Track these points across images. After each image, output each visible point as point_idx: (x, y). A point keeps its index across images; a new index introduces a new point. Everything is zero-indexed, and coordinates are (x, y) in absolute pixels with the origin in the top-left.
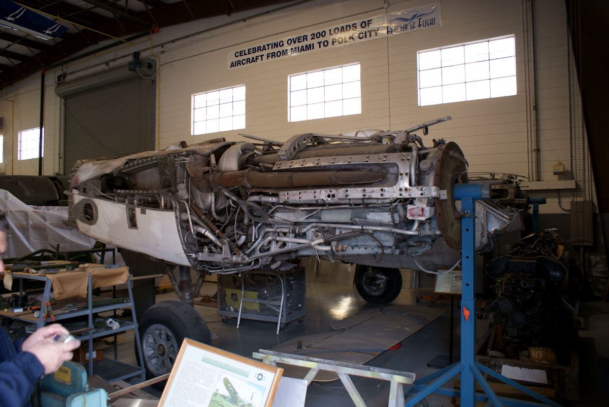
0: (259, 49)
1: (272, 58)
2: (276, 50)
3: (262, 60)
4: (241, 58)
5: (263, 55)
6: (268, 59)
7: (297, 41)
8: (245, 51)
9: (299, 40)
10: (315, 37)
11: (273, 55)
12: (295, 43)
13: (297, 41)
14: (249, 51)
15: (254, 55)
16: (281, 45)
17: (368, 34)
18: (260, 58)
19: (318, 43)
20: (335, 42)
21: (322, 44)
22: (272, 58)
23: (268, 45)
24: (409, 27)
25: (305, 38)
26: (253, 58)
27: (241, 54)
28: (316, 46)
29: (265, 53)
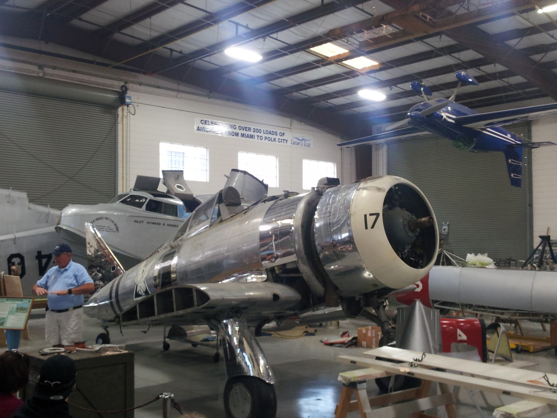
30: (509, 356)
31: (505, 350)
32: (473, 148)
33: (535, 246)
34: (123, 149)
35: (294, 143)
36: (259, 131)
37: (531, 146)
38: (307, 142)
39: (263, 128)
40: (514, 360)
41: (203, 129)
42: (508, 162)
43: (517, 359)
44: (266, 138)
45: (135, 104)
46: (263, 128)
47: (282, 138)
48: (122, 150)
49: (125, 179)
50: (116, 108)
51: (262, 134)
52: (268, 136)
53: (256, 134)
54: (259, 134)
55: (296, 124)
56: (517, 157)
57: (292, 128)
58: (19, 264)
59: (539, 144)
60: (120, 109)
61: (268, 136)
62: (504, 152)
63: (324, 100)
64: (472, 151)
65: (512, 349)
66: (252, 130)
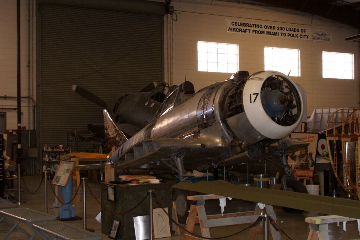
0: (247, 25)
1: (256, 33)
2: (258, 29)
3: (249, 33)
4: (236, 27)
5: (250, 30)
6: (253, 33)
7: (270, 28)
8: (238, 23)
9: (270, 27)
10: (279, 29)
11: (256, 32)
13: (270, 28)
14: (241, 24)
15: (245, 28)
16: (261, 27)
17: (304, 36)
18: (248, 31)
19: (308, 36)
20: (289, 35)
21: (283, 34)
22: (256, 33)
23: (253, 25)
24: (320, 39)
25: (274, 28)
26: (244, 29)
27: (236, 24)
28: (251, 31)
29: (252, 29)
36: (283, 29)
38: (326, 37)
44: (289, 35)
45: (177, 13)
47: (303, 34)
49: (169, 73)
50: (161, 17)
51: (285, 31)
53: (280, 32)
54: (282, 31)
57: (312, 25)
60: (165, 17)
66: (276, 28)
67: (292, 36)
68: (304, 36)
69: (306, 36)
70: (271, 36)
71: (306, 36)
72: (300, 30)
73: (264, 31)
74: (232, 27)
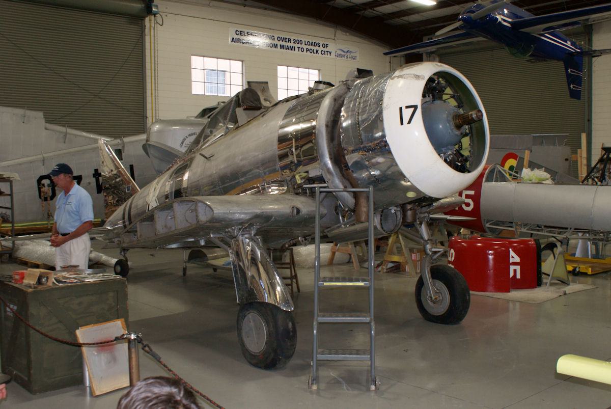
9: (285, 40)
12: (283, 41)
21: (300, 49)
24: (345, 57)
25: (289, 40)
30: (566, 279)
31: (561, 273)
32: (530, 56)
33: (593, 165)
34: (151, 63)
35: (339, 55)
36: (300, 42)
37: (593, 54)
39: (304, 39)
40: (571, 283)
41: (239, 41)
42: (567, 72)
43: (574, 282)
44: (307, 50)
45: (164, 15)
46: (304, 39)
47: (325, 49)
48: (150, 64)
49: (154, 95)
50: (142, 19)
51: (303, 46)
52: (309, 47)
53: (296, 45)
55: (340, 34)
56: (578, 66)
58: (49, 186)
59: (602, 52)
60: (147, 19)
61: (309, 47)
62: (564, 62)
63: (371, 8)
64: (528, 61)
65: (569, 272)
66: (292, 41)
67: (312, 51)
68: (326, 53)
69: (328, 53)
70: (285, 50)
71: (328, 53)
72: (321, 45)
73: (277, 45)
74: (236, 37)
